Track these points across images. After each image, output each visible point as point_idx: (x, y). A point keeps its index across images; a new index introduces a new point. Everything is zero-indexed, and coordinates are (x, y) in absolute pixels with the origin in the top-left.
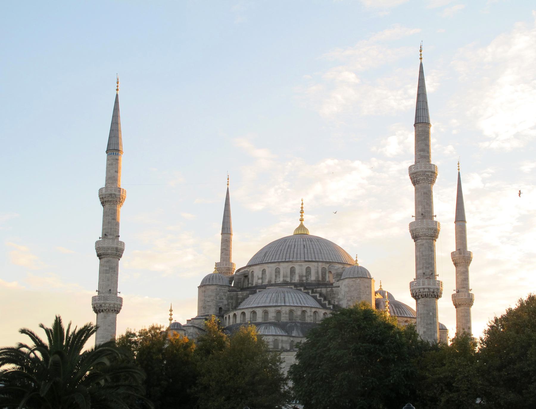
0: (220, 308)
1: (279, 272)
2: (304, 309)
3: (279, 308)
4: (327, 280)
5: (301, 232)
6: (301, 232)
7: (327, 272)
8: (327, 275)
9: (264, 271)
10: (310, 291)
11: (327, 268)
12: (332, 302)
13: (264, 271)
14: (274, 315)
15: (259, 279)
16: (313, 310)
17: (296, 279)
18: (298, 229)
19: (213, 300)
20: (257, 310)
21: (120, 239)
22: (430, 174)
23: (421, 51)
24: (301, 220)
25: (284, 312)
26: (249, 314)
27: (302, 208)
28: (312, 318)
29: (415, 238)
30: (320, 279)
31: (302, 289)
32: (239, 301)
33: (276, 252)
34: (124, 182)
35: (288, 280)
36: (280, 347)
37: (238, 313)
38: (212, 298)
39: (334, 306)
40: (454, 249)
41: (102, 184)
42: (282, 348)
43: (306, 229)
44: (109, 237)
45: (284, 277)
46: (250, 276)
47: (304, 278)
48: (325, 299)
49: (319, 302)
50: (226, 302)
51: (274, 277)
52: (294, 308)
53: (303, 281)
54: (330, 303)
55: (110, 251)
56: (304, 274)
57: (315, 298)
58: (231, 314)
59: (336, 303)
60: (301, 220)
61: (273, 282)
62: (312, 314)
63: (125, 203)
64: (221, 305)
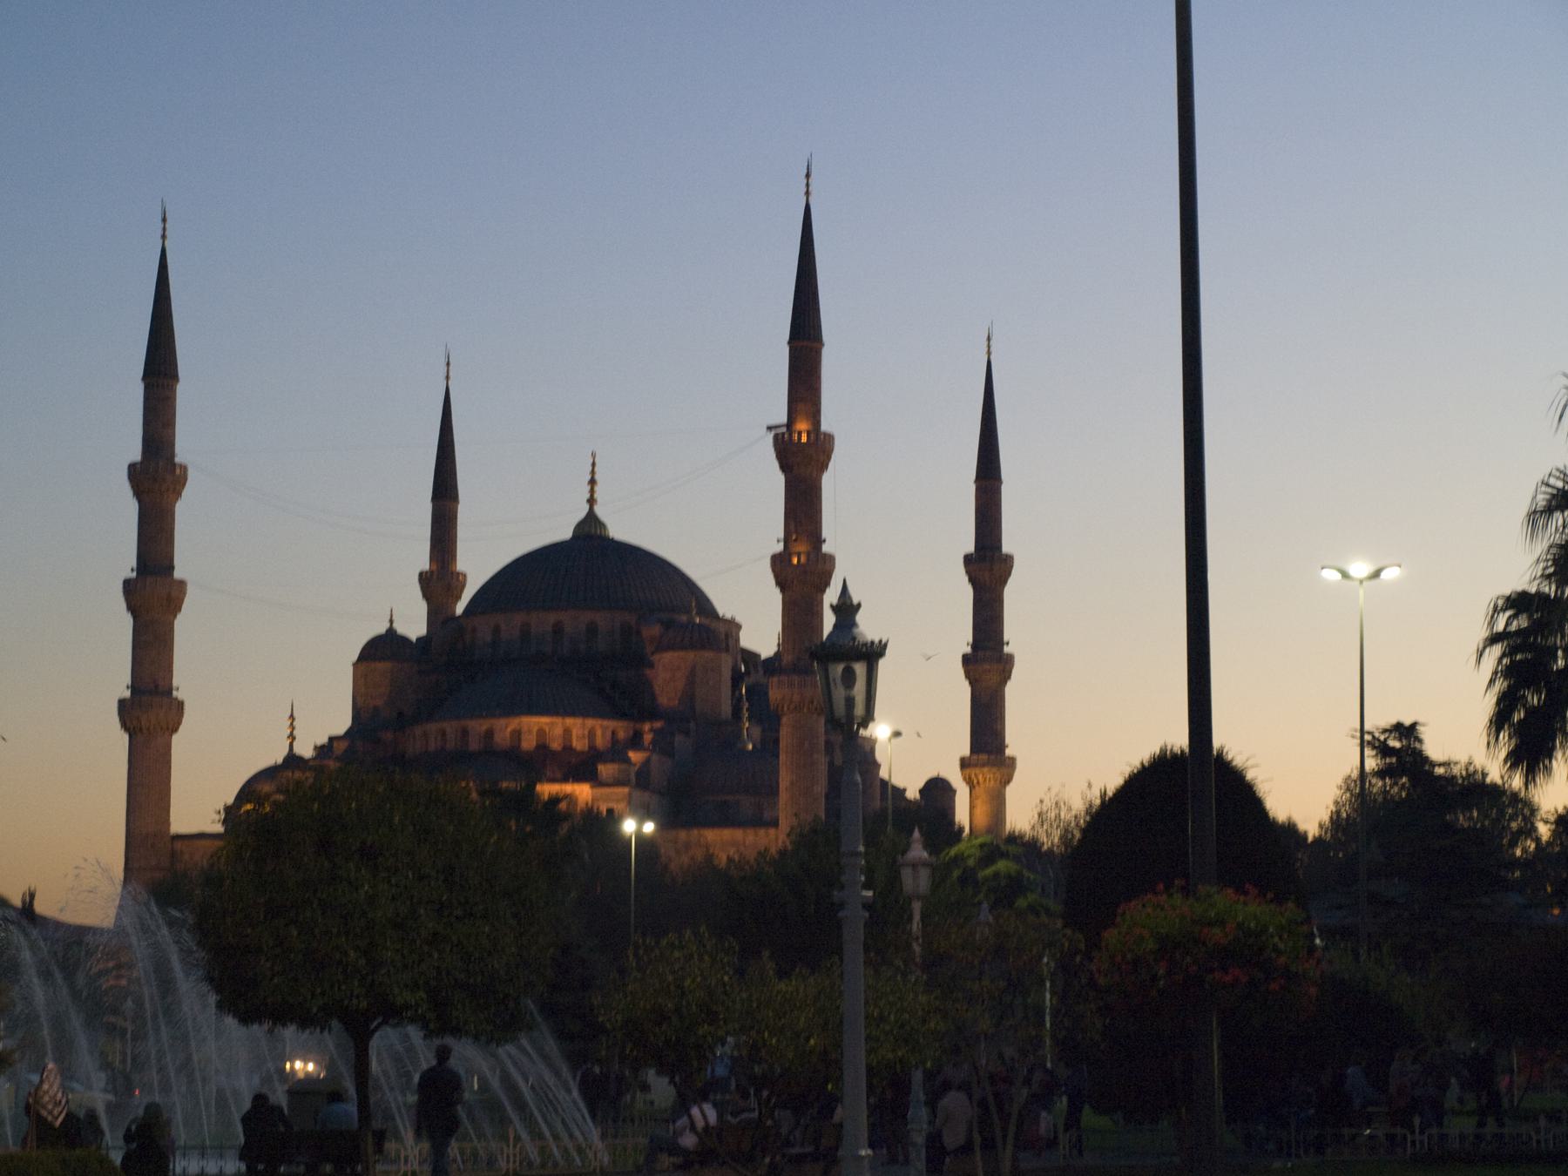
5: (590, 529)
6: (590, 529)
9: (497, 630)
13: (497, 630)
18: (580, 526)
21: (178, 574)
23: (808, 176)
24: (591, 501)
27: (593, 472)
29: (781, 583)
33: (528, 577)
34: (185, 448)
37: (432, 727)
40: (970, 547)
41: (136, 454)
43: (602, 525)
58: (418, 730)
60: (591, 501)
63: (187, 492)
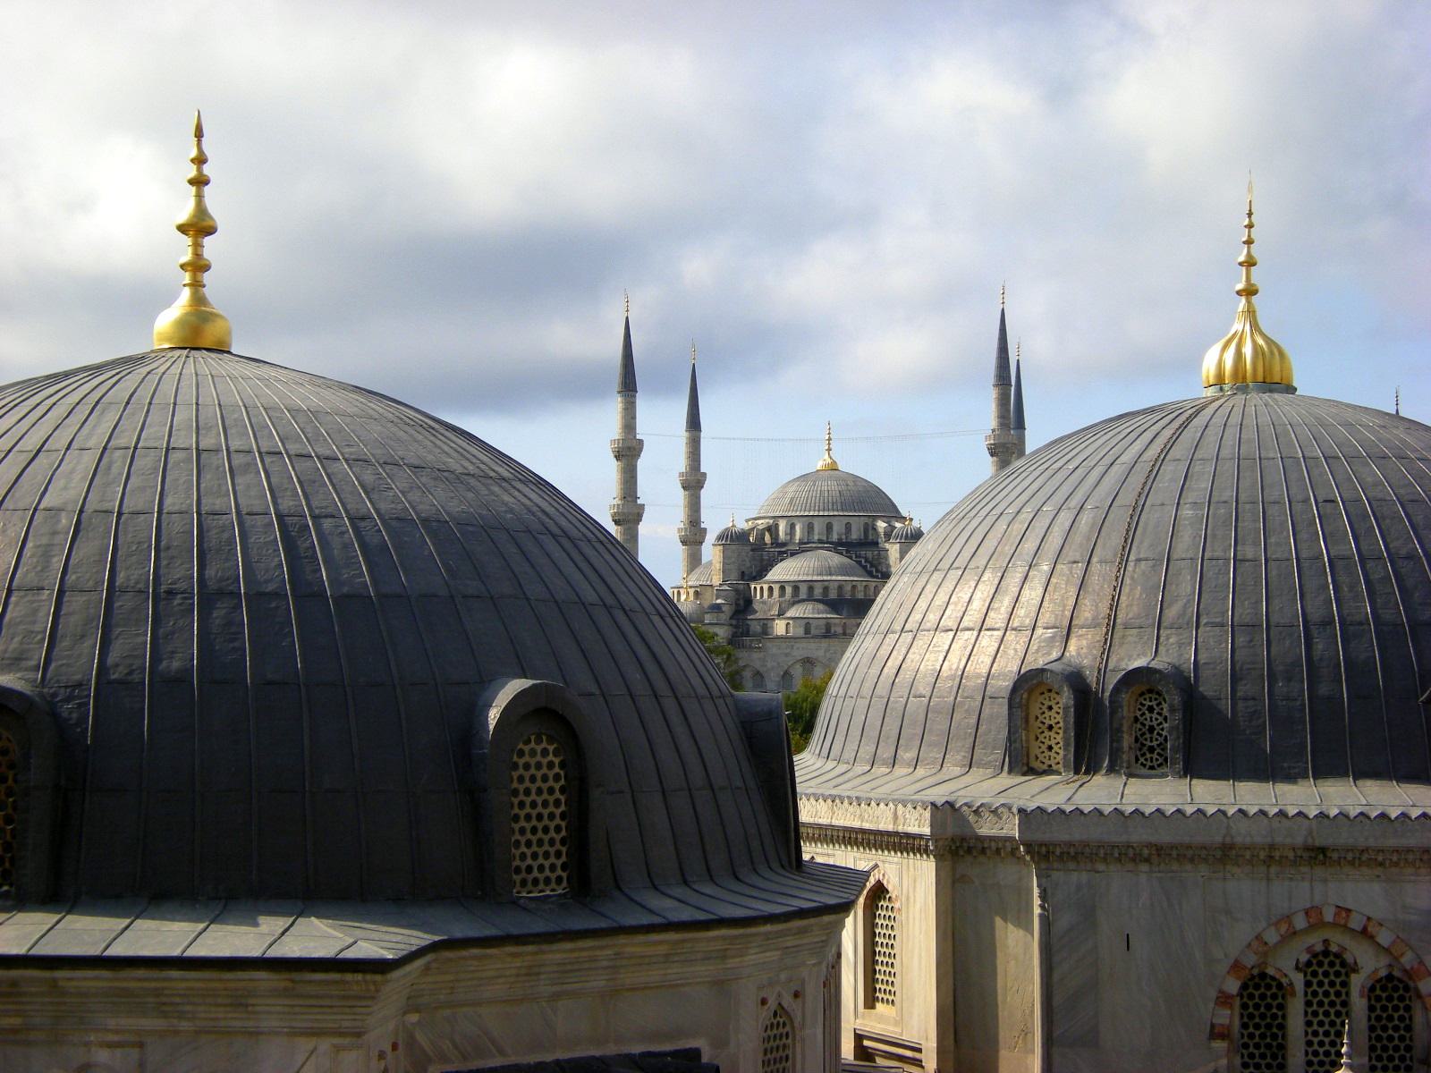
0: (743, 572)
1: (812, 528)
2: (854, 583)
3: (826, 583)
4: (870, 537)
7: (870, 529)
8: (871, 532)
10: (854, 556)
11: (870, 523)
12: (880, 568)
14: (821, 590)
15: (786, 534)
16: (864, 584)
17: (835, 537)
19: (734, 562)
20: (801, 585)
21: (639, 502)
22: (1010, 445)
25: (832, 587)
26: (791, 589)
28: (862, 593)
30: (862, 537)
31: (844, 553)
32: (765, 563)
35: (825, 538)
36: (832, 631)
38: (733, 559)
39: (882, 573)
42: (835, 632)
44: (630, 499)
45: (819, 534)
46: (773, 529)
47: (844, 537)
48: (872, 566)
49: (864, 568)
50: (748, 564)
51: (806, 534)
52: (844, 583)
53: (842, 539)
54: (877, 571)
55: (631, 517)
56: (844, 531)
57: (859, 563)
59: (884, 570)
61: (806, 541)
62: (863, 589)
64: (743, 569)
